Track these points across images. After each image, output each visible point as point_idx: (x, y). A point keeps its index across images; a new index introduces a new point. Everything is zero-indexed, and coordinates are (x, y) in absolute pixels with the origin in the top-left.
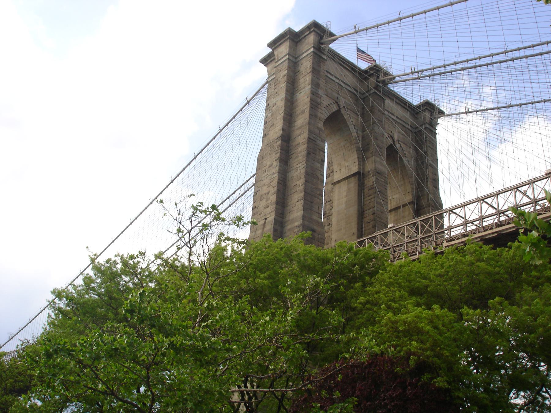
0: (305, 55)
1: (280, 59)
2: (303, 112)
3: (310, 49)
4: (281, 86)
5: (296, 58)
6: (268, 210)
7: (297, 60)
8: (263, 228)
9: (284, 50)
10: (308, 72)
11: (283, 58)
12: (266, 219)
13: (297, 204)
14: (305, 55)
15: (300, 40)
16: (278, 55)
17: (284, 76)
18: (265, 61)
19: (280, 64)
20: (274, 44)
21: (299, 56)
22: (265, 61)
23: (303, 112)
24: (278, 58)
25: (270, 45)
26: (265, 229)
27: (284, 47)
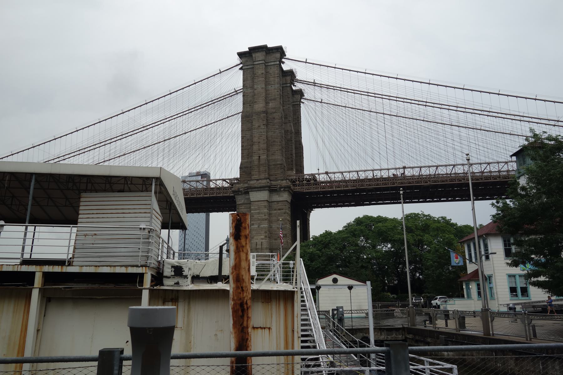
0: (272, 63)
1: (258, 61)
2: (275, 99)
3: (277, 61)
4: (260, 79)
5: (266, 63)
6: (261, 152)
7: (267, 64)
8: (259, 162)
9: (259, 56)
10: (277, 75)
11: (260, 61)
12: (259, 157)
13: (276, 151)
14: (272, 63)
15: (269, 53)
16: (255, 57)
17: (262, 74)
18: (241, 55)
19: (258, 64)
20: (253, 50)
21: (268, 62)
22: (241, 55)
23: (275, 99)
24: (255, 59)
25: (249, 48)
26: (260, 162)
27: (260, 54)
